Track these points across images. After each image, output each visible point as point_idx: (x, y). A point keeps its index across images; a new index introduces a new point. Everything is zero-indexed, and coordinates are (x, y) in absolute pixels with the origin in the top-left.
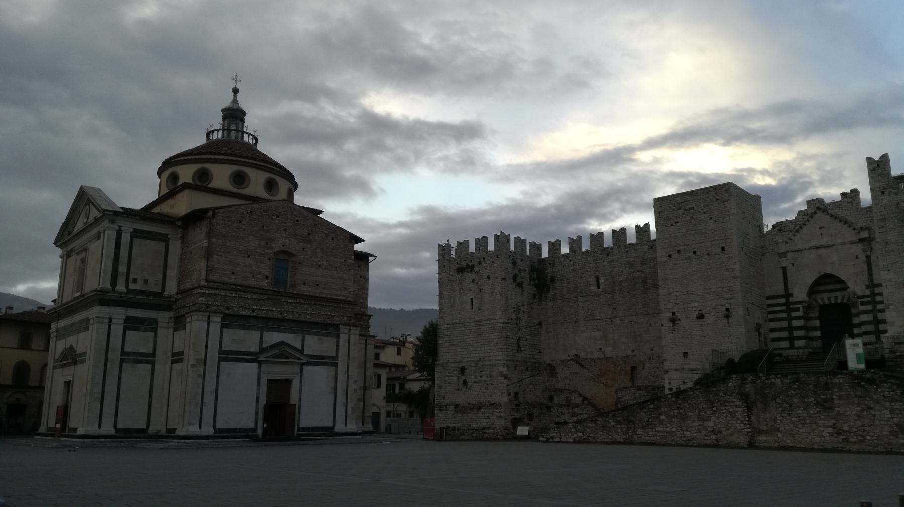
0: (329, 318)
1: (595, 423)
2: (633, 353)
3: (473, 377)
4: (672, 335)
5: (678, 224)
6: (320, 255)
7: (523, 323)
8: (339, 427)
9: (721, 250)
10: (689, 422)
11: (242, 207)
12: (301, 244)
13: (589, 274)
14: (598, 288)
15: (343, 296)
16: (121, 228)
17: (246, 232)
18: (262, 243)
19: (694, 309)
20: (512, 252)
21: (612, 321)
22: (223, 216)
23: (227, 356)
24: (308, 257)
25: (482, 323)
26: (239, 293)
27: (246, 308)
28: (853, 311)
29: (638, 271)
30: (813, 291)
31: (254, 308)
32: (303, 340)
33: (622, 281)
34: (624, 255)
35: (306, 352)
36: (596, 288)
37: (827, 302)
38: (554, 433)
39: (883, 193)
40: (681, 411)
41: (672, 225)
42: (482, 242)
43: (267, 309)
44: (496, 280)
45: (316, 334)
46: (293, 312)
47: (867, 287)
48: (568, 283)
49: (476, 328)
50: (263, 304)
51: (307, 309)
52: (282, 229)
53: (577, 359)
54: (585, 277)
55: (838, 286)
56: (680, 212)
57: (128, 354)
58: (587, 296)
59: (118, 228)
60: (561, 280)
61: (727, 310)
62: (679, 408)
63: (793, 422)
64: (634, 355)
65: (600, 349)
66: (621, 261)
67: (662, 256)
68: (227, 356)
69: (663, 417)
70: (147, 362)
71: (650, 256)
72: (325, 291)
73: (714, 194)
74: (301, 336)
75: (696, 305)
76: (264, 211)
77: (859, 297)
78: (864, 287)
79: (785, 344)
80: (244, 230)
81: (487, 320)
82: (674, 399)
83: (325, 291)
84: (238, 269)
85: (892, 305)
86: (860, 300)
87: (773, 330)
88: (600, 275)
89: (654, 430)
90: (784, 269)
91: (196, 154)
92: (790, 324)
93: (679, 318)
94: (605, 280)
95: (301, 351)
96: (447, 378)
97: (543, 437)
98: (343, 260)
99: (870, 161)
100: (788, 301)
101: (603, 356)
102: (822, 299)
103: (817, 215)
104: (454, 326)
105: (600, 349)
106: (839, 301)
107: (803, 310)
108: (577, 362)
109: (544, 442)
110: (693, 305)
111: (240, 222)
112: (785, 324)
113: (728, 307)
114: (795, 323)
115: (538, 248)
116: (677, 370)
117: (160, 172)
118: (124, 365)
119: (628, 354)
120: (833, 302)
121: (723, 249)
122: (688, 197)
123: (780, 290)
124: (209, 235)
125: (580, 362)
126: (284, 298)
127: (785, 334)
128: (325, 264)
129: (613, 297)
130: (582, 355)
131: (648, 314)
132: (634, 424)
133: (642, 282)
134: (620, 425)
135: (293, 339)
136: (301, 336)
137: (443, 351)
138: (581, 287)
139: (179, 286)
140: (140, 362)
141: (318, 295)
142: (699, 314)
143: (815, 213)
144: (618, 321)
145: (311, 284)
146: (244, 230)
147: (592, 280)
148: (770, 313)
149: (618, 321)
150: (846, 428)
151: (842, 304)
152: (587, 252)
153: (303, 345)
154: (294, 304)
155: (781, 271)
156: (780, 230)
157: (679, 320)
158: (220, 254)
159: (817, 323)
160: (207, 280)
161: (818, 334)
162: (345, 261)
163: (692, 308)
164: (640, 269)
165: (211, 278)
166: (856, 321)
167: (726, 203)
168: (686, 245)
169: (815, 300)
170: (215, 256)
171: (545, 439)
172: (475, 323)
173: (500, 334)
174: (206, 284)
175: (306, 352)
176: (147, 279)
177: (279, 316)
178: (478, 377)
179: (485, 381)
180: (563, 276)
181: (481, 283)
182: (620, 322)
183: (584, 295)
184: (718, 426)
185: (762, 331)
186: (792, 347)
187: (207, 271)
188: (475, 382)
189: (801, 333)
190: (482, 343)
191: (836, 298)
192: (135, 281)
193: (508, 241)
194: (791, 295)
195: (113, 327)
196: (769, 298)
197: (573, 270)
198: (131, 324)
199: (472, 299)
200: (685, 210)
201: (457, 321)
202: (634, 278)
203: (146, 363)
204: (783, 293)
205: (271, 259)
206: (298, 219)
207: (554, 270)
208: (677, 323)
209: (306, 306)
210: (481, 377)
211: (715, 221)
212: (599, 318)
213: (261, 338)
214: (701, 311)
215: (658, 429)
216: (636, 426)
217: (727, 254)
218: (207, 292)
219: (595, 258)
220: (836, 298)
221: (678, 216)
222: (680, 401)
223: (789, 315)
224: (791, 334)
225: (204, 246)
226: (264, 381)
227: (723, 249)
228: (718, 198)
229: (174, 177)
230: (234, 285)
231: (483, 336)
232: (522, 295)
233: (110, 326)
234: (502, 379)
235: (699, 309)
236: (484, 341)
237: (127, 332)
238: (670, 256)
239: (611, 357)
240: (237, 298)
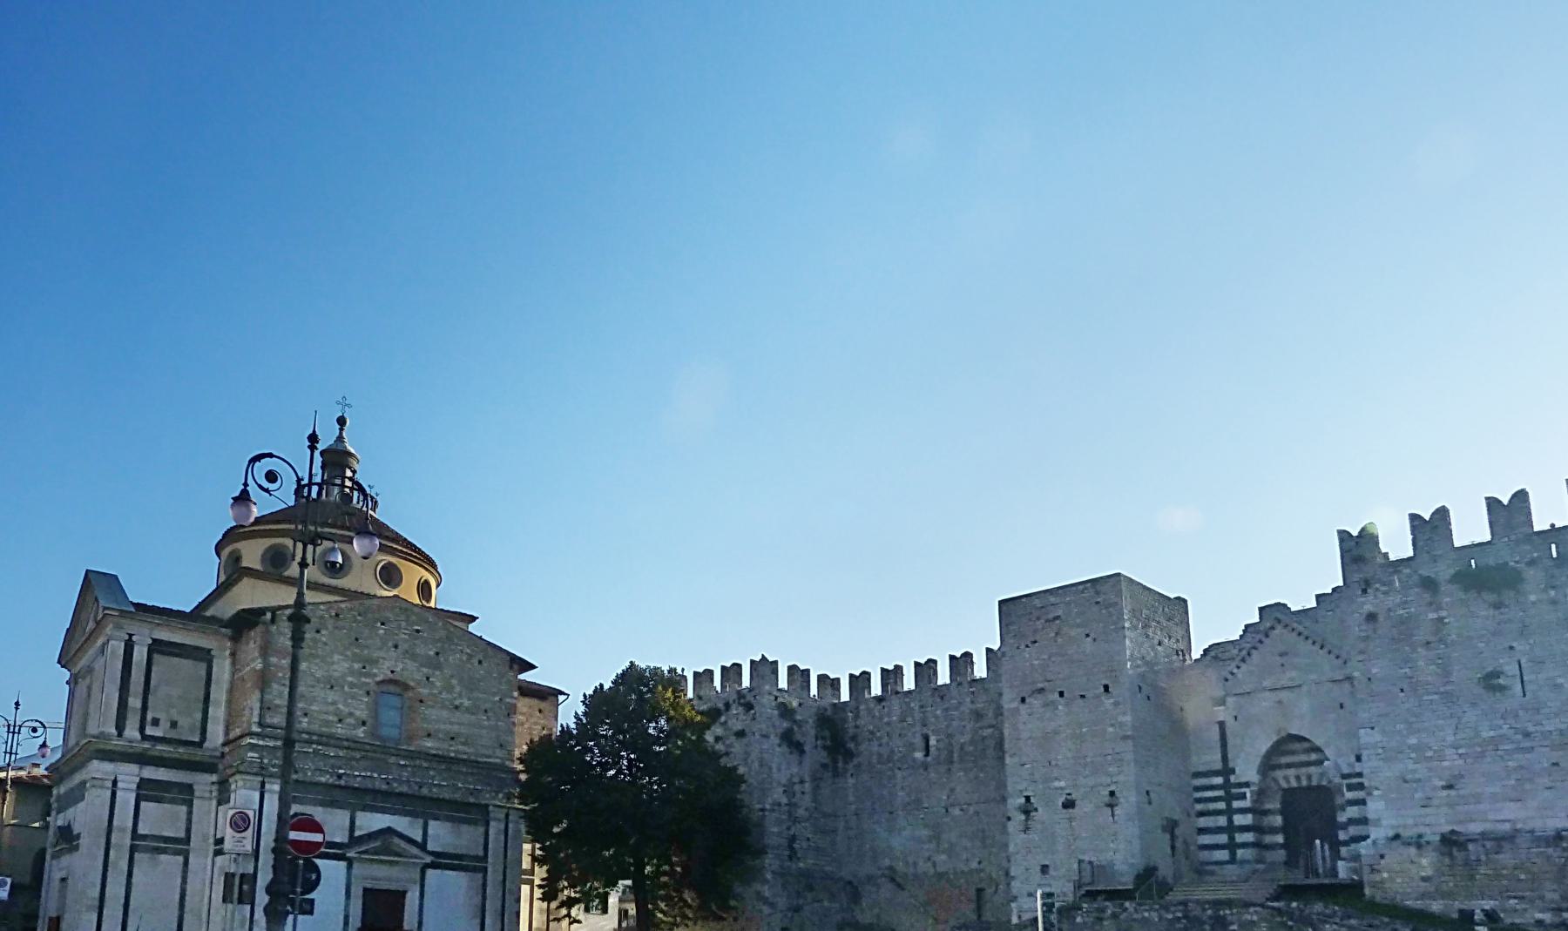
2: (982, 866)
4: (1026, 836)
5: (1037, 644)
6: (458, 689)
7: (801, 812)
9: (1102, 690)
19: (1060, 792)
20: (780, 690)
24: (435, 691)
26: (314, 746)
27: (328, 772)
28: (1339, 801)
30: (1268, 765)
31: (341, 771)
37: (1294, 784)
41: (1027, 646)
43: (363, 774)
46: (408, 781)
48: (880, 745)
50: (357, 765)
51: (433, 778)
53: (893, 877)
55: (1314, 757)
56: (1039, 624)
60: (869, 740)
61: (1112, 794)
64: (982, 870)
72: (465, 749)
73: (1092, 594)
75: (1062, 784)
77: (1344, 777)
79: (1223, 855)
83: (465, 749)
84: (313, 708)
85: (1377, 789)
86: (1345, 782)
87: (1202, 831)
88: (930, 734)
90: (1222, 725)
91: (268, 523)
92: (1230, 821)
93: (1035, 806)
94: (938, 741)
98: (497, 698)
99: (1344, 536)
100: (1227, 781)
101: (932, 871)
102: (1286, 778)
107: (1251, 796)
108: (893, 880)
110: (1057, 784)
112: (1222, 821)
113: (1113, 788)
114: (1239, 820)
115: (832, 685)
117: (218, 549)
118: (137, 855)
121: (1106, 688)
122: (1052, 599)
123: (1214, 760)
126: (393, 758)
127: (1223, 838)
129: (950, 770)
138: (900, 752)
139: (227, 733)
141: (452, 755)
142: (1066, 799)
143: (1273, 628)
145: (440, 736)
147: (918, 741)
148: (1199, 801)
149: (956, 812)
151: (1319, 787)
152: (910, 692)
155: (1217, 728)
156: (1216, 658)
157: (1036, 810)
159: (1278, 820)
160: (260, 724)
161: (1280, 839)
162: (501, 699)
163: (1056, 788)
165: (268, 720)
166: (1342, 818)
167: (1111, 609)
168: (1049, 681)
169: (1275, 780)
174: (259, 730)
176: (175, 719)
177: (384, 787)
185: (1178, 832)
186: (1233, 860)
187: (261, 709)
189: (1249, 837)
193: (775, 672)
194: (1233, 771)
196: (1197, 775)
200: (1047, 621)
202: (984, 738)
204: (1218, 766)
205: (371, 693)
208: (1032, 814)
211: (1095, 640)
212: (926, 805)
214: (1069, 794)
217: (1112, 697)
218: (261, 743)
221: (1035, 631)
223: (1229, 805)
224: (1232, 838)
225: (258, 668)
227: (1106, 688)
228: (1099, 600)
229: (236, 558)
230: (308, 733)
232: (800, 763)
233: (114, 794)
235: (1068, 792)
237: (143, 804)
240: (312, 755)
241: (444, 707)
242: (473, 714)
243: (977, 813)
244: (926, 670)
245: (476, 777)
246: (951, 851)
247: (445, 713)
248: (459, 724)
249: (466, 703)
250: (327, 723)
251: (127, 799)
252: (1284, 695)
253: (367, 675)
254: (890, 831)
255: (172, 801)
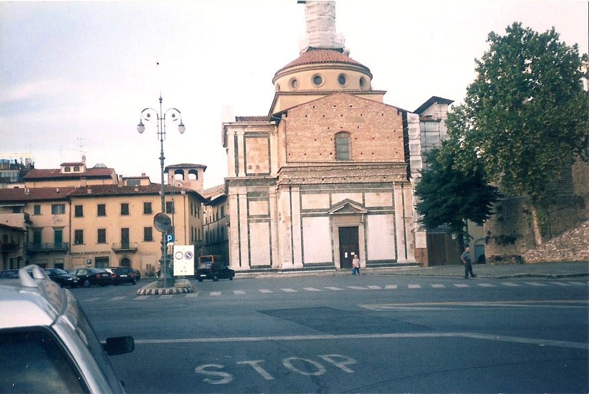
0: (384, 178)
8: (399, 261)
11: (307, 105)
12: (356, 123)
15: (395, 159)
17: (311, 122)
18: (325, 128)
22: (293, 114)
23: (306, 213)
26: (310, 168)
31: (323, 177)
32: (363, 197)
35: (366, 206)
45: (373, 191)
51: (365, 173)
52: (339, 115)
57: (253, 216)
68: (306, 213)
70: (267, 221)
74: (361, 194)
76: (324, 104)
80: (311, 121)
89: (580, 252)
95: (363, 206)
111: (306, 116)
124: (285, 130)
128: (377, 136)
134: (560, 249)
135: (356, 197)
136: (361, 194)
140: (261, 221)
146: (311, 121)
153: (364, 200)
154: (354, 171)
158: (294, 142)
170: (291, 144)
175: (366, 206)
192: (250, 167)
195: (240, 200)
198: (251, 197)
203: (265, 222)
206: (351, 105)
209: (364, 171)
213: (330, 199)
215: (582, 251)
226: (336, 230)
237: (250, 202)
241: (367, 139)
242: (381, 140)
245: (386, 170)
247: (367, 143)
248: (375, 146)
249: (378, 135)
250: (315, 157)
251: (243, 200)
253: (329, 131)
255: (262, 199)
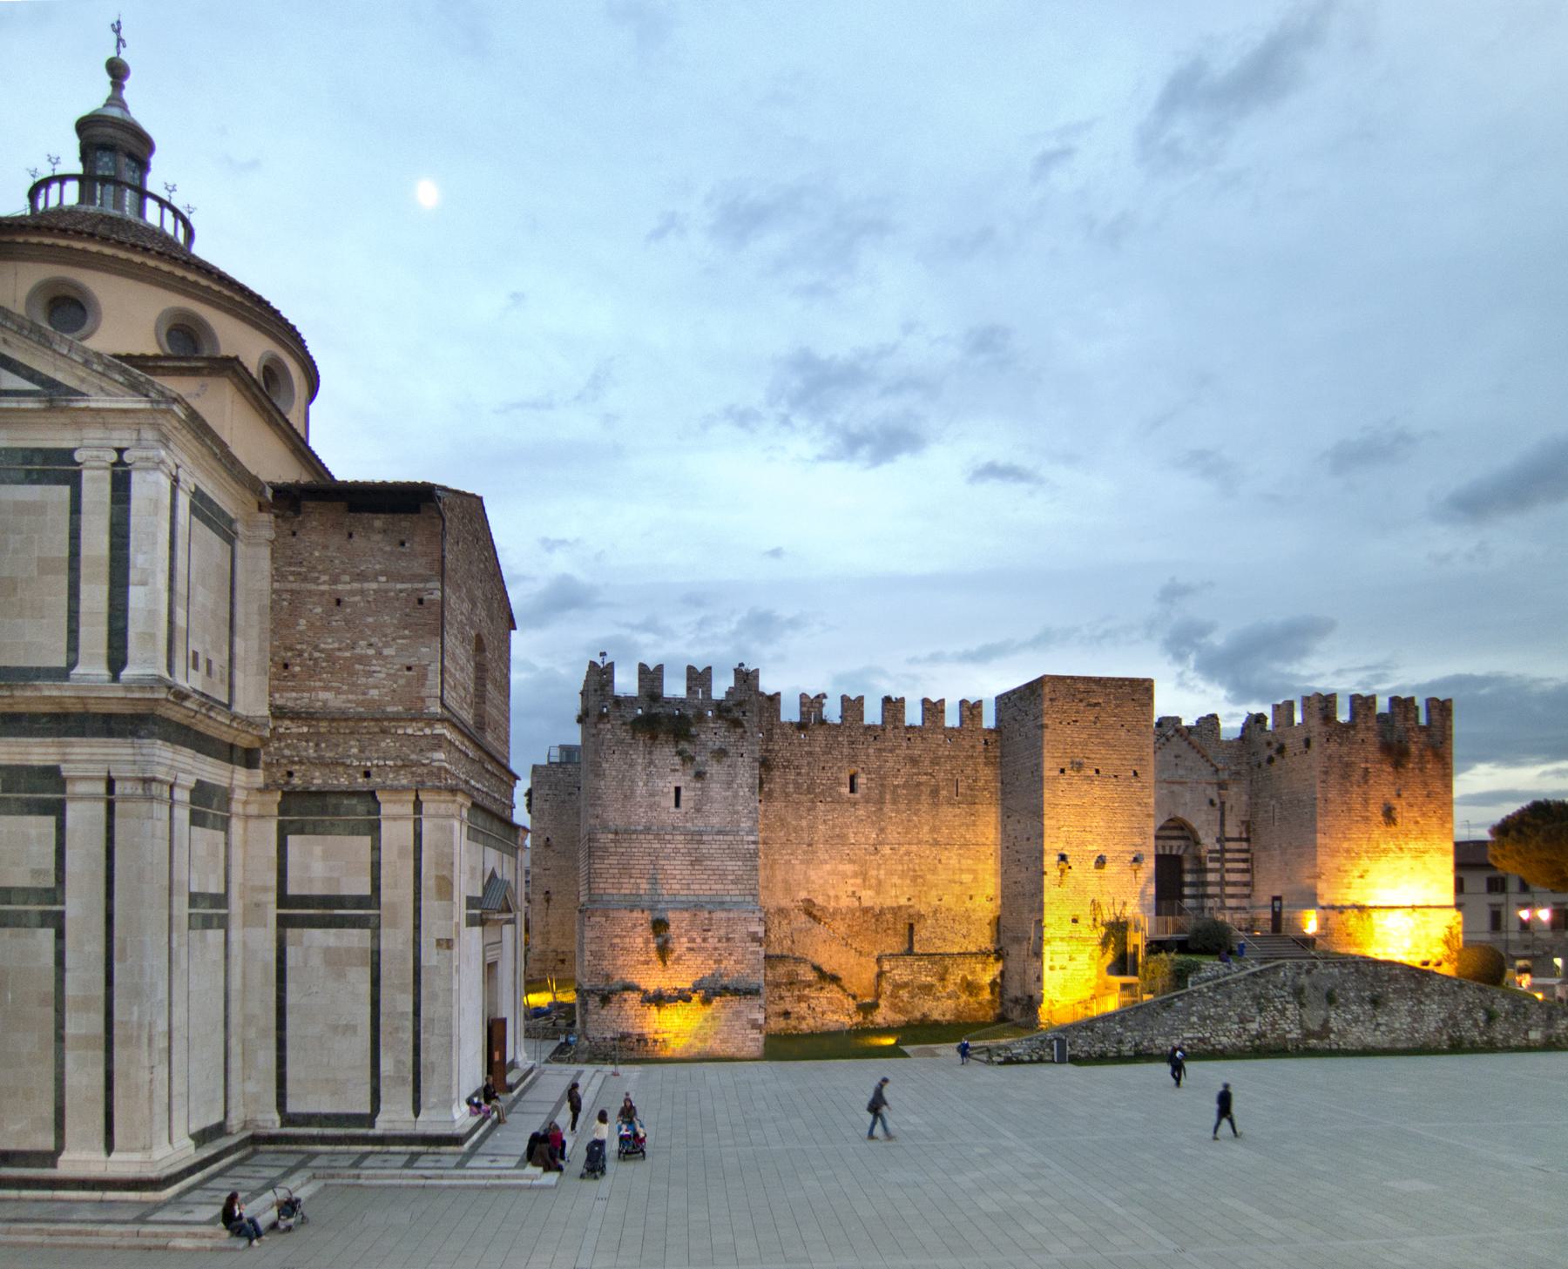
1: (1092, 1031)
2: (911, 903)
3: (684, 940)
10: (1228, 1024)
13: (840, 764)
14: (852, 790)
16: (127, 457)
21: (876, 849)
25: (705, 838)
29: (926, 774)
33: (898, 786)
34: (904, 744)
36: (848, 789)
38: (1020, 1048)
39: (1328, 740)
40: (1219, 1009)
42: (698, 678)
44: (740, 759)
47: (1218, 840)
48: (799, 774)
49: (690, 846)
54: (830, 768)
58: (832, 802)
59: (114, 457)
60: (784, 767)
62: (1216, 1006)
63: (1345, 1020)
64: (910, 906)
65: (854, 893)
66: (897, 751)
67: (1051, 769)
69: (1194, 1019)
71: (947, 753)
78: (1214, 840)
81: (719, 833)
82: (1210, 994)
96: (616, 941)
97: (999, 1055)
103: (1175, 739)
104: (634, 836)
105: (854, 893)
106: (1174, 852)
108: (810, 914)
109: (1000, 1063)
116: (1062, 939)
119: (902, 903)
120: (1167, 852)
122: (1095, 687)
125: (815, 912)
129: (881, 809)
130: (819, 901)
131: (936, 843)
132: (1152, 1030)
133: (932, 791)
137: (602, 885)
138: (823, 784)
144: (886, 850)
149: (886, 850)
150: (1397, 1025)
164: (930, 771)
171: (1002, 1059)
172: (689, 837)
173: (749, 863)
178: (699, 940)
179: (716, 949)
180: (788, 761)
181: (704, 759)
182: (890, 852)
183: (829, 799)
184: (1264, 1028)
188: (690, 949)
190: (706, 877)
191: (1171, 848)
197: (810, 753)
199: (678, 790)
201: (641, 828)
202: (919, 784)
207: (770, 747)
210: (704, 940)
212: (853, 841)
215: (1186, 1035)
216: (1155, 1032)
219: (853, 739)
220: (1171, 848)
222: (1218, 997)
231: (705, 863)
234: (754, 947)
236: (710, 872)
238: (1062, 771)
239: (872, 908)
243: (908, 853)
244: (853, 706)
246: (879, 887)
252: (1176, 788)
254: (808, 862)
